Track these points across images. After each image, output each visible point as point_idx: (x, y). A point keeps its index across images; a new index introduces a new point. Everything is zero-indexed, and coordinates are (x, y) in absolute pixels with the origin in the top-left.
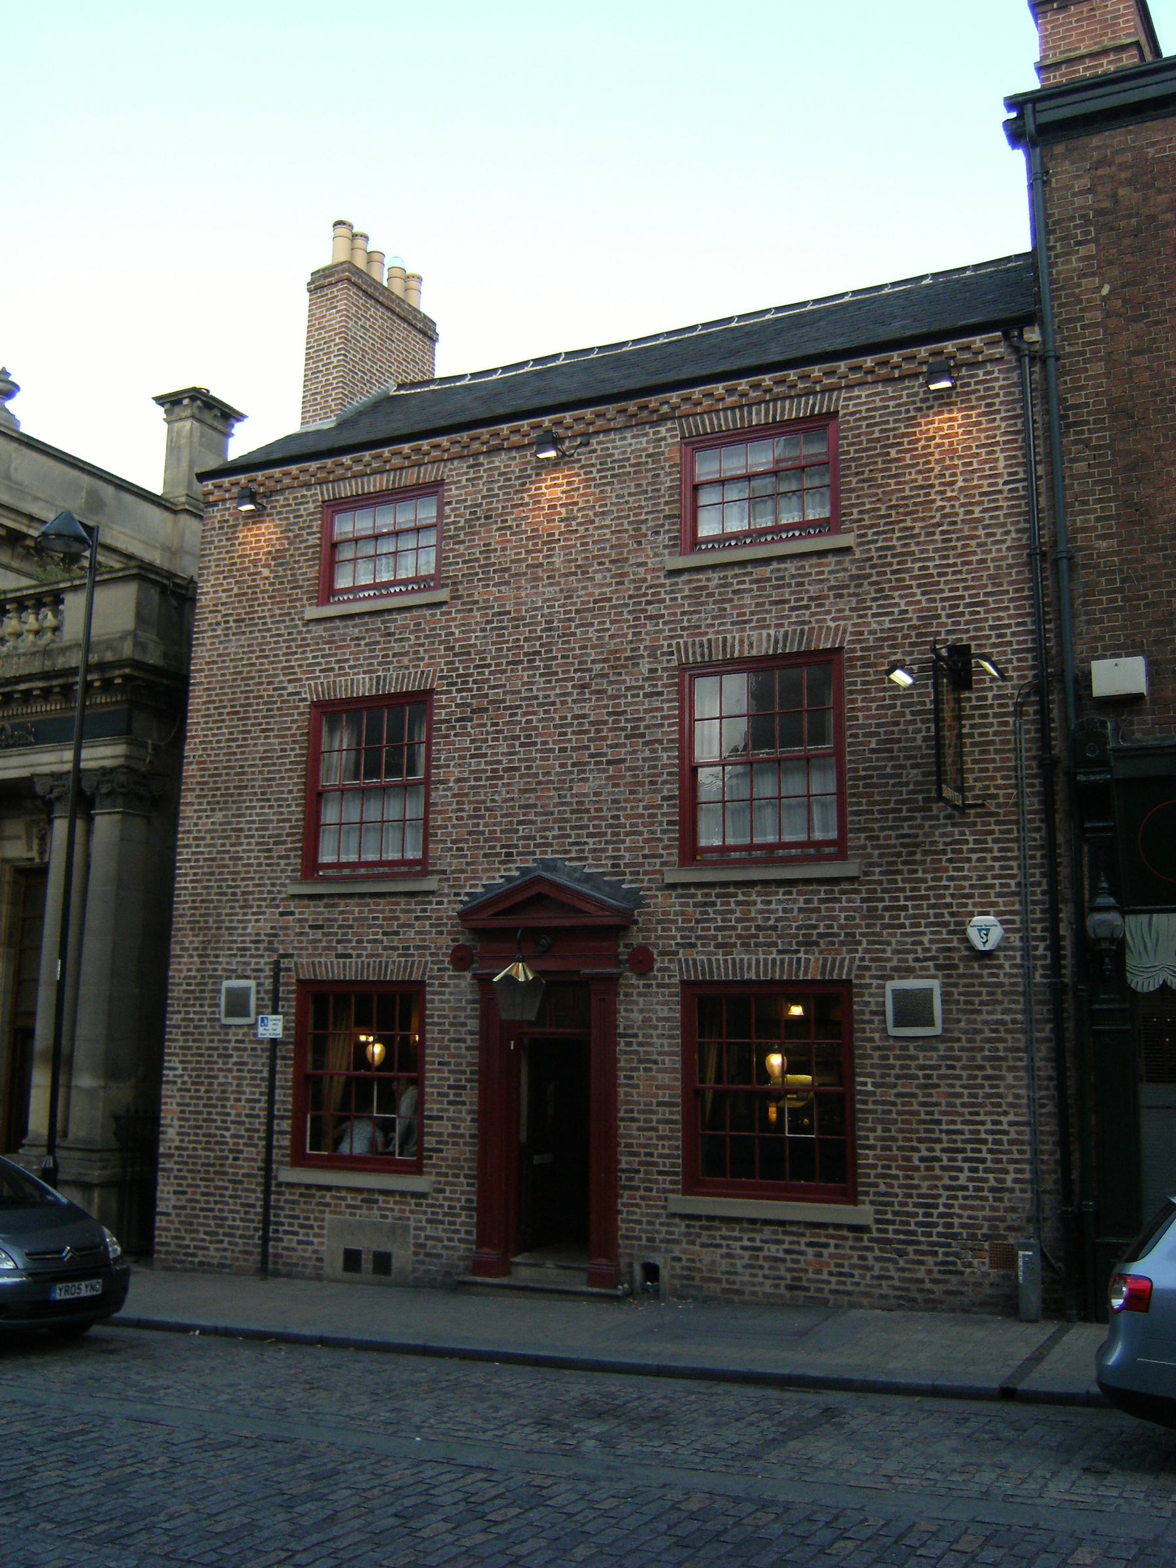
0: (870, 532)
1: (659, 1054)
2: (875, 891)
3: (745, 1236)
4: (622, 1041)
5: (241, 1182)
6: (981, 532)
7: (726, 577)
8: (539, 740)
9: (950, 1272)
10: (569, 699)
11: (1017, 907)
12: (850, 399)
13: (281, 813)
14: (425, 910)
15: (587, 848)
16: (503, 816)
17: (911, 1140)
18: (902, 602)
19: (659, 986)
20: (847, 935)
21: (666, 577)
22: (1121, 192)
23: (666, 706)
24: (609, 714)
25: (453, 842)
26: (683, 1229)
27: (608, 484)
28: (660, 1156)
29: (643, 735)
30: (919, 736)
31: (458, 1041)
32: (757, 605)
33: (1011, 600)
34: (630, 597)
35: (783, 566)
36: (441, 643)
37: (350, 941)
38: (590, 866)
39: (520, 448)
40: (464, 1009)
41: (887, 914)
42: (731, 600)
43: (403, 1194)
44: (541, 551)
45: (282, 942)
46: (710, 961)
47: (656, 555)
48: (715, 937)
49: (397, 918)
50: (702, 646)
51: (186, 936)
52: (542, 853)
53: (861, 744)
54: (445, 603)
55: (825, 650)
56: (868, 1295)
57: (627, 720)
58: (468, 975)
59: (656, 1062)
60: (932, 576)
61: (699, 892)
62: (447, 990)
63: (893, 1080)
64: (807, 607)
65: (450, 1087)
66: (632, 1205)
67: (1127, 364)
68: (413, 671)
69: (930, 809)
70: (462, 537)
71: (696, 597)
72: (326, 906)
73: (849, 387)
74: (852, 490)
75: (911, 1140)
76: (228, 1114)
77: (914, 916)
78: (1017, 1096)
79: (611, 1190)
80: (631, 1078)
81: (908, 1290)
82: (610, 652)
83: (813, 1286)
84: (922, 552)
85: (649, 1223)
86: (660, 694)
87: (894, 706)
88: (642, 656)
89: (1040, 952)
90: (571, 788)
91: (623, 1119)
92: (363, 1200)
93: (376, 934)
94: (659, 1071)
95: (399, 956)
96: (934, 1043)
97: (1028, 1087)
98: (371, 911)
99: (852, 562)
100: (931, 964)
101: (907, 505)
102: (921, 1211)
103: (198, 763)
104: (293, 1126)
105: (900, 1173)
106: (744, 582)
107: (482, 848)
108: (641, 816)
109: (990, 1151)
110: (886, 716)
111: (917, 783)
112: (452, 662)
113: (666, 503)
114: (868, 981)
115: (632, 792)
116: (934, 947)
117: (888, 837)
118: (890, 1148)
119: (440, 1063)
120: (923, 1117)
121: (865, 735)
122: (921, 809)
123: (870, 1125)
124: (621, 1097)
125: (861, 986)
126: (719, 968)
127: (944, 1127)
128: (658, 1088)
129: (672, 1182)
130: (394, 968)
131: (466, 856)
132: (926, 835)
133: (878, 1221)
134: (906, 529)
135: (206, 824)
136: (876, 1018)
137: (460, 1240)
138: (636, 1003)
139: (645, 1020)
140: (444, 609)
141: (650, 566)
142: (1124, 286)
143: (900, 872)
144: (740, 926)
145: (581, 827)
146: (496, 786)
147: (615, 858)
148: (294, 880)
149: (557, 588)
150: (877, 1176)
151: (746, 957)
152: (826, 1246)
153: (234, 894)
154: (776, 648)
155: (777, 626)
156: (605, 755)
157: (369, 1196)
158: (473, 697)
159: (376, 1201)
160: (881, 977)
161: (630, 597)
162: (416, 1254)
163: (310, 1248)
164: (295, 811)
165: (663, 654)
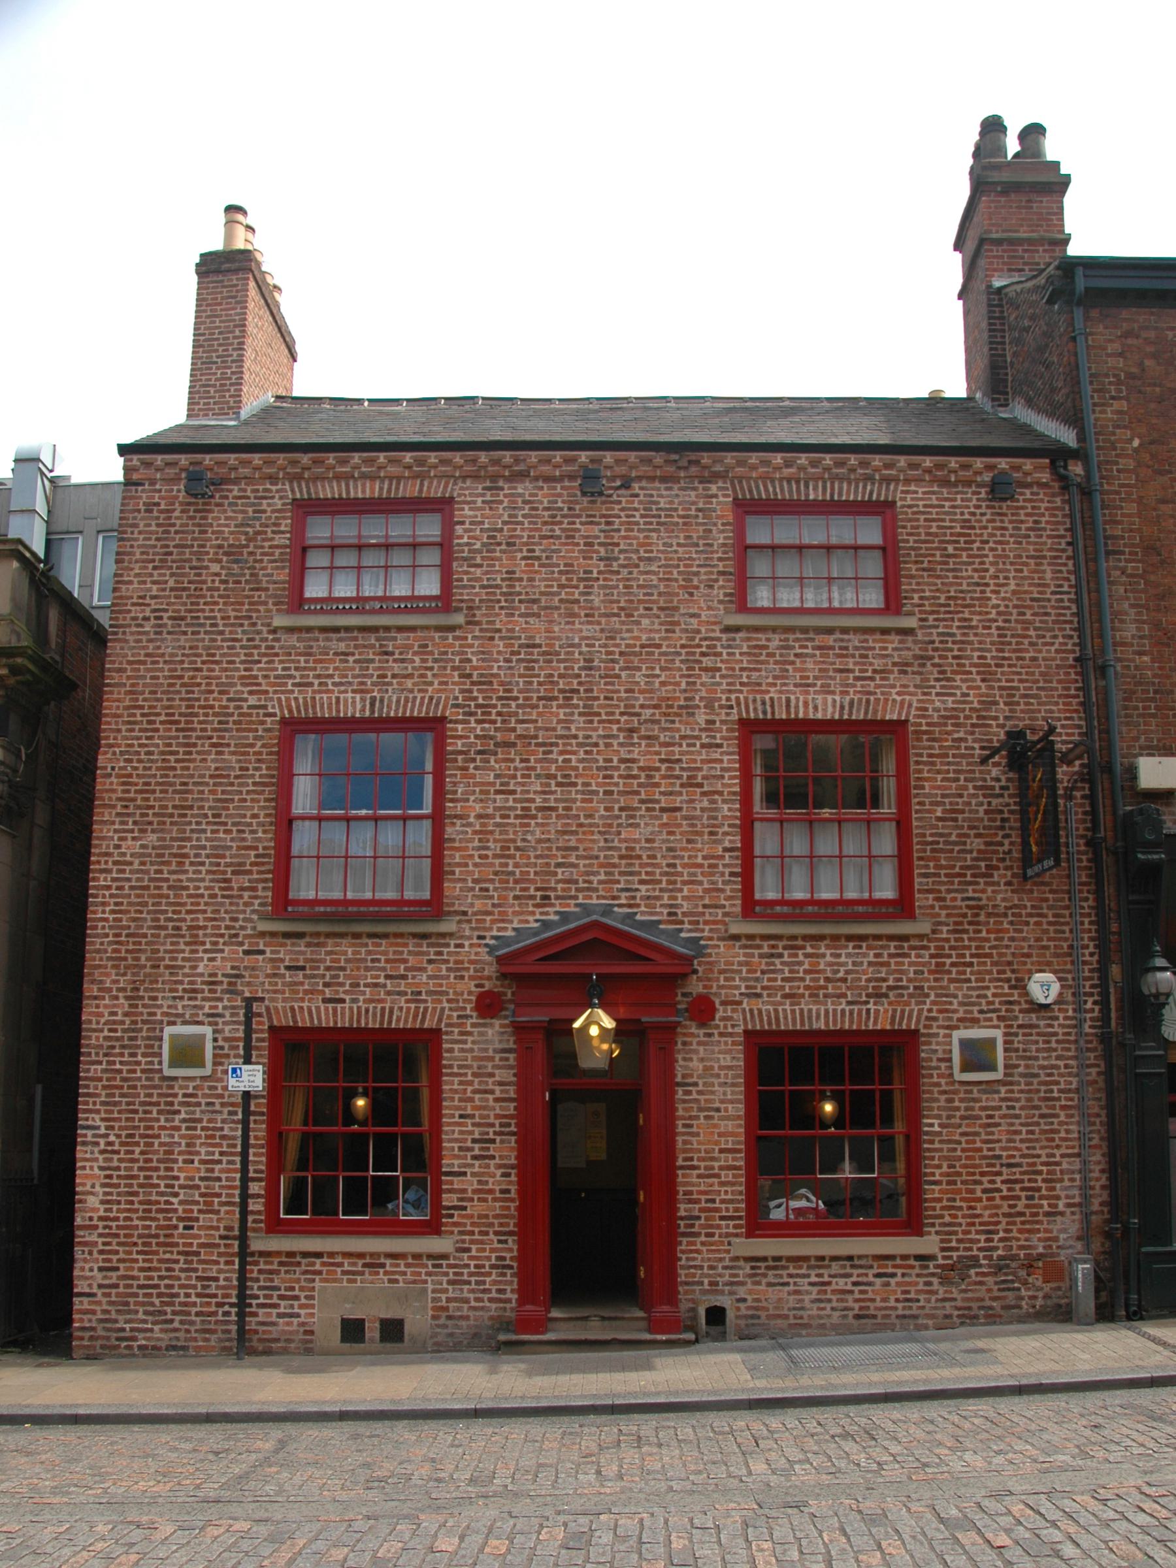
0: (931, 617)
1: (722, 1102)
2: (943, 948)
3: (813, 1273)
4: (680, 1090)
5: (198, 1254)
6: (1032, 633)
7: (787, 640)
8: (580, 781)
9: (1009, 1289)
10: (615, 742)
11: (1069, 967)
12: (907, 492)
13: (244, 839)
14: (440, 953)
15: (638, 895)
16: (536, 857)
17: (974, 1174)
18: (964, 686)
19: (721, 1034)
20: (915, 988)
21: (722, 631)
22: (1147, 363)
23: (726, 758)
24: (662, 761)
25: (475, 881)
26: (748, 1271)
27: (654, 530)
28: (723, 1201)
29: (701, 785)
30: (981, 809)
31: (486, 1092)
32: (820, 670)
33: (1060, 696)
34: (683, 646)
35: (846, 637)
36: (454, 669)
37: (342, 985)
38: (643, 913)
39: (548, 479)
40: (492, 1059)
41: (954, 970)
42: (793, 663)
43: (417, 1256)
44: (577, 587)
45: (249, 984)
46: (776, 1011)
47: (709, 608)
48: (783, 988)
49: (405, 961)
50: (764, 703)
51: (108, 975)
52: (585, 898)
53: (929, 811)
54: (460, 627)
55: (891, 722)
56: (932, 1317)
57: (682, 769)
58: (497, 1023)
59: (718, 1110)
60: (989, 666)
61: (765, 944)
62: (470, 1039)
63: (958, 1121)
64: (872, 679)
65: (474, 1141)
66: (691, 1251)
67: (1155, 509)
68: (419, 696)
69: (992, 876)
70: (479, 561)
71: (755, 655)
72: (308, 945)
73: (907, 481)
74: (912, 577)
75: (974, 1174)
76: (177, 1178)
77: (979, 972)
78: (1067, 1131)
79: (671, 1237)
80: (691, 1126)
81: (970, 1308)
82: (661, 699)
83: (880, 1313)
84: (980, 643)
85: (711, 1268)
86: (719, 746)
87: (958, 780)
88: (698, 707)
89: (1089, 1006)
90: (619, 833)
91: (682, 1168)
92: (365, 1265)
93: (378, 977)
94: (721, 1118)
95: (407, 1001)
96: (996, 1087)
97: (1078, 1123)
98: (369, 953)
99: (915, 642)
100: (994, 1015)
101: (964, 599)
102: (983, 1237)
103: (118, 776)
104: (267, 1189)
105: (964, 1205)
106: (806, 647)
107: (512, 889)
108: (701, 866)
109: (1044, 1181)
110: (950, 788)
111: (979, 851)
112: (471, 691)
113: (720, 559)
114: (934, 1031)
115: (689, 841)
116: (997, 1000)
117: (954, 899)
118: (955, 1183)
119: (461, 1116)
120: (985, 1153)
121: (931, 804)
122: (984, 875)
123: (936, 1162)
124: (680, 1145)
125: (929, 1035)
126: (786, 1018)
127: (1004, 1161)
128: (720, 1135)
129: (735, 1227)
130: (402, 1015)
131: (492, 897)
132: (988, 899)
133: (943, 1249)
134: (965, 620)
135: (131, 847)
136: (943, 1065)
137: (491, 1300)
138: (696, 1052)
139: (706, 1069)
140: (457, 633)
141: (703, 618)
142: (1152, 443)
143: (966, 931)
144: (808, 977)
145: (631, 874)
146: (528, 825)
147: (671, 906)
148: (264, 917)
149: (597, 628)
150: (943, 1208)
151: (814, 1008)
152: (893, 1275)
153: (178, 928)
154: (841, 714)
155: (842, 693)
156: (658, 802)
157: (373, 1263)
158: (496, 730)
159: (383, 1266)
160: (948, 1027)
161: (683, 646)
162: (434, 1317)
163: (295, 1320)
164: (264, 838)
165: (721, 707)
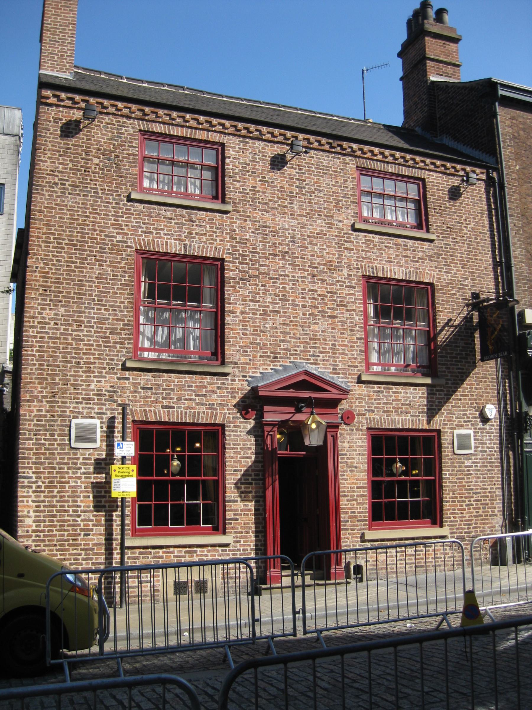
5: (92, 549)
6: (480, 248)
10: (306, 280)
13: (116, 315)
14: (224, 384)
16: (271, 336)
19: (357, 430)
23: (357, 293)
24: (328, 292)
28: (359, 513)
29: (346, 306)
37: (172, 398)
38: (321, 368)
46: (381, 419)
51: (36, 388)
62: (239, 430)
64: (418, 262)
68: (210, 246)
69: (467, 359)
70: (238, 179)
75: (462, 497)
76: (79, 506)
86: (354, 287)
90: (309, 327)
100: (469, 423)
102: (466, 527)
105: (459, 512)
108: (347, 346)
109: (489, 500)
111: (463, 347)
115: (341, 333)
119: (235, 471)
120: (467, 487)
122: (464, 358)
127: (474, 491)
133: (451, 533)
140: (228, 215)
145: (315, 348)
147: (334, 365)
149: (296, 221)
151: (397, 418)
